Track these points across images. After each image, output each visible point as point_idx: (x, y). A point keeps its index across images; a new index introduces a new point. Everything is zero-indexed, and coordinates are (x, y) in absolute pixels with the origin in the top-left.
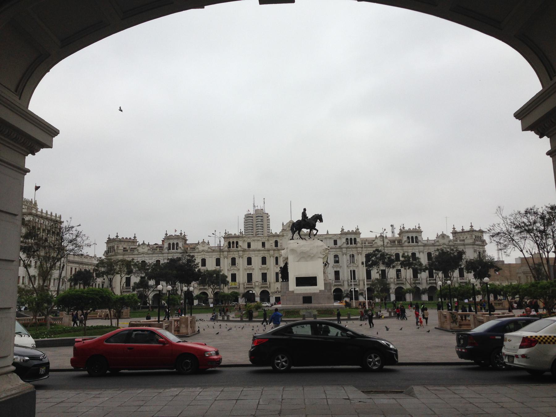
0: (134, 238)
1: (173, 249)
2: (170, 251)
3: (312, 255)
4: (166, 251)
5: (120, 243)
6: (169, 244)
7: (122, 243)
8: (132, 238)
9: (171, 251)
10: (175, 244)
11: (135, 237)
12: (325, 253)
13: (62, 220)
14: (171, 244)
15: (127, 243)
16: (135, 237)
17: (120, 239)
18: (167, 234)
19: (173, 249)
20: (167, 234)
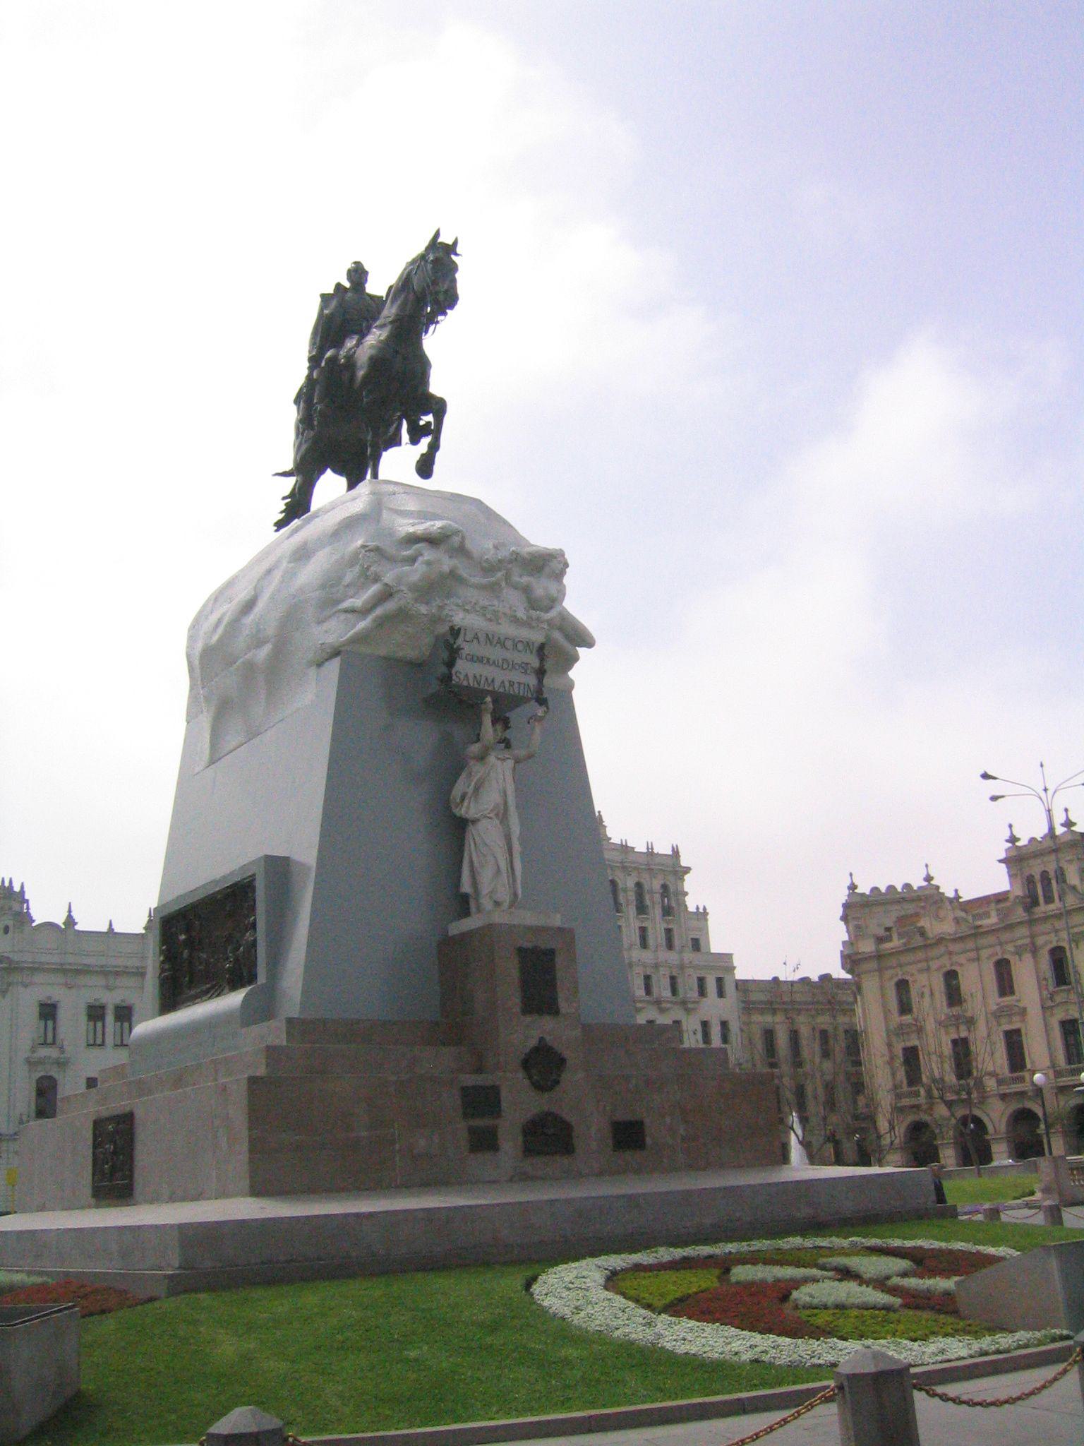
0: (925, 884)
1: (1049, 900)
2: (1036, 910)
3: (263, 653)
4: (1020, 914)
5: (867, 910)
6: (1030, 880)
7: (876, 909)
8: (918, 882)
9: (1042, 909)
10: (1052, 874)
11: (928, 878)
12: (374, 589)
13: (684, 863)
14: (1037, 877)
15: (897, 907)
16: (928, 878)
17: (863, 895)
18: (1018, 839)
19: (1049, 900)
20: (1018, 839)
